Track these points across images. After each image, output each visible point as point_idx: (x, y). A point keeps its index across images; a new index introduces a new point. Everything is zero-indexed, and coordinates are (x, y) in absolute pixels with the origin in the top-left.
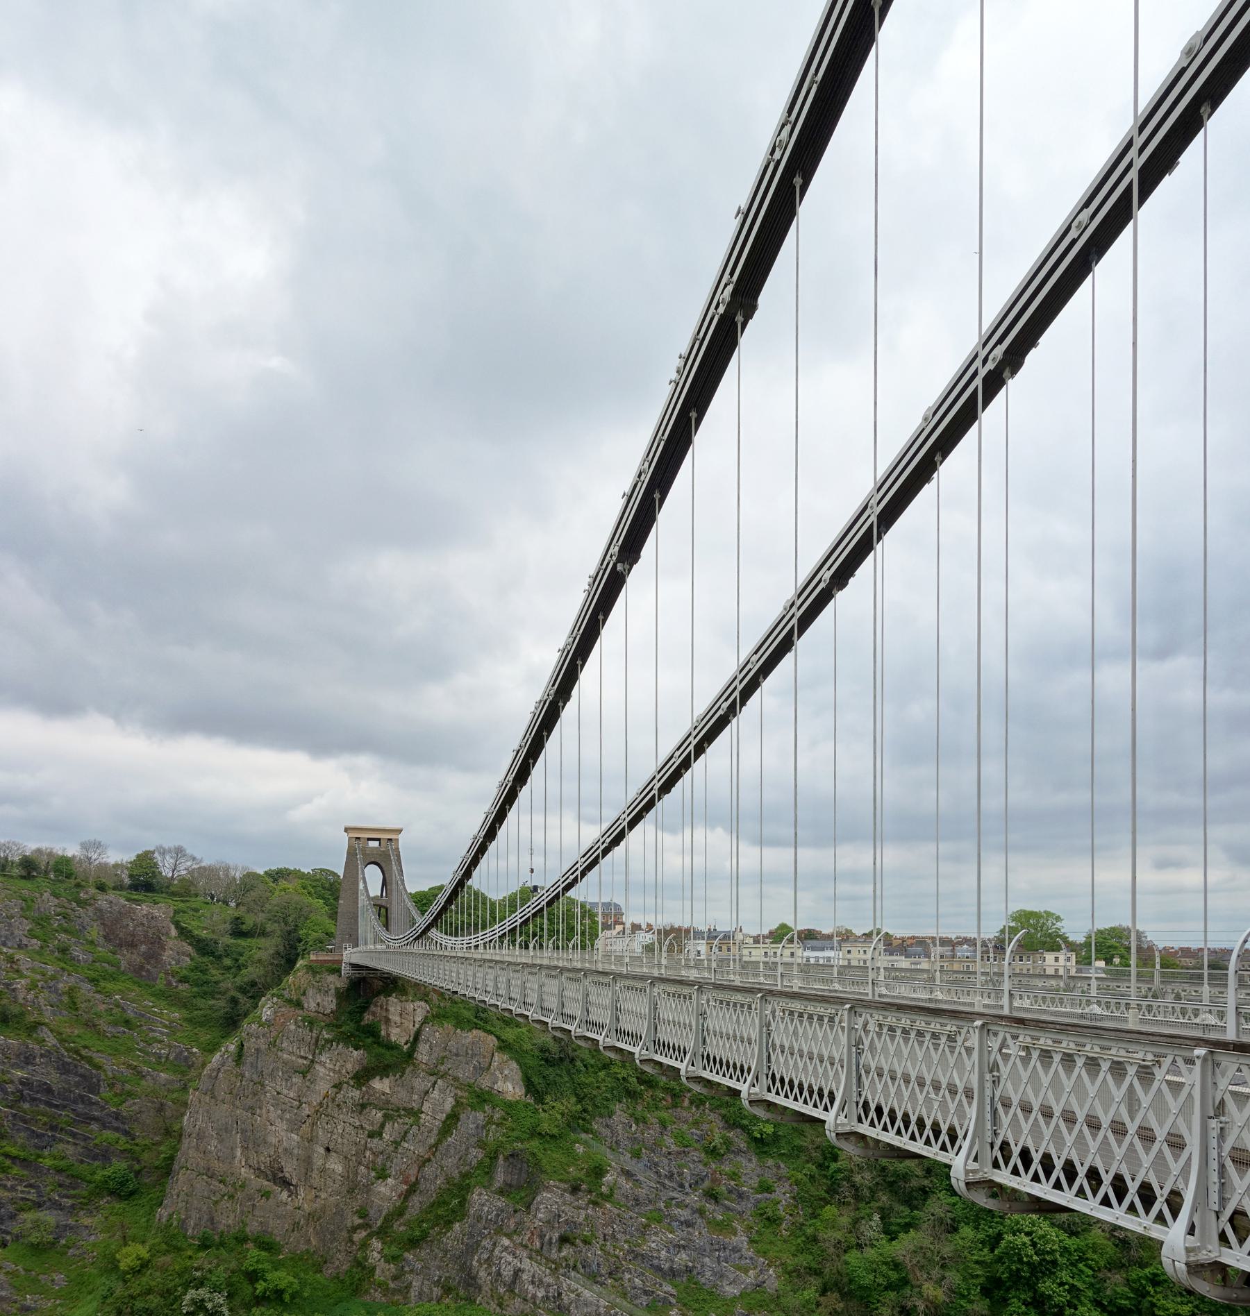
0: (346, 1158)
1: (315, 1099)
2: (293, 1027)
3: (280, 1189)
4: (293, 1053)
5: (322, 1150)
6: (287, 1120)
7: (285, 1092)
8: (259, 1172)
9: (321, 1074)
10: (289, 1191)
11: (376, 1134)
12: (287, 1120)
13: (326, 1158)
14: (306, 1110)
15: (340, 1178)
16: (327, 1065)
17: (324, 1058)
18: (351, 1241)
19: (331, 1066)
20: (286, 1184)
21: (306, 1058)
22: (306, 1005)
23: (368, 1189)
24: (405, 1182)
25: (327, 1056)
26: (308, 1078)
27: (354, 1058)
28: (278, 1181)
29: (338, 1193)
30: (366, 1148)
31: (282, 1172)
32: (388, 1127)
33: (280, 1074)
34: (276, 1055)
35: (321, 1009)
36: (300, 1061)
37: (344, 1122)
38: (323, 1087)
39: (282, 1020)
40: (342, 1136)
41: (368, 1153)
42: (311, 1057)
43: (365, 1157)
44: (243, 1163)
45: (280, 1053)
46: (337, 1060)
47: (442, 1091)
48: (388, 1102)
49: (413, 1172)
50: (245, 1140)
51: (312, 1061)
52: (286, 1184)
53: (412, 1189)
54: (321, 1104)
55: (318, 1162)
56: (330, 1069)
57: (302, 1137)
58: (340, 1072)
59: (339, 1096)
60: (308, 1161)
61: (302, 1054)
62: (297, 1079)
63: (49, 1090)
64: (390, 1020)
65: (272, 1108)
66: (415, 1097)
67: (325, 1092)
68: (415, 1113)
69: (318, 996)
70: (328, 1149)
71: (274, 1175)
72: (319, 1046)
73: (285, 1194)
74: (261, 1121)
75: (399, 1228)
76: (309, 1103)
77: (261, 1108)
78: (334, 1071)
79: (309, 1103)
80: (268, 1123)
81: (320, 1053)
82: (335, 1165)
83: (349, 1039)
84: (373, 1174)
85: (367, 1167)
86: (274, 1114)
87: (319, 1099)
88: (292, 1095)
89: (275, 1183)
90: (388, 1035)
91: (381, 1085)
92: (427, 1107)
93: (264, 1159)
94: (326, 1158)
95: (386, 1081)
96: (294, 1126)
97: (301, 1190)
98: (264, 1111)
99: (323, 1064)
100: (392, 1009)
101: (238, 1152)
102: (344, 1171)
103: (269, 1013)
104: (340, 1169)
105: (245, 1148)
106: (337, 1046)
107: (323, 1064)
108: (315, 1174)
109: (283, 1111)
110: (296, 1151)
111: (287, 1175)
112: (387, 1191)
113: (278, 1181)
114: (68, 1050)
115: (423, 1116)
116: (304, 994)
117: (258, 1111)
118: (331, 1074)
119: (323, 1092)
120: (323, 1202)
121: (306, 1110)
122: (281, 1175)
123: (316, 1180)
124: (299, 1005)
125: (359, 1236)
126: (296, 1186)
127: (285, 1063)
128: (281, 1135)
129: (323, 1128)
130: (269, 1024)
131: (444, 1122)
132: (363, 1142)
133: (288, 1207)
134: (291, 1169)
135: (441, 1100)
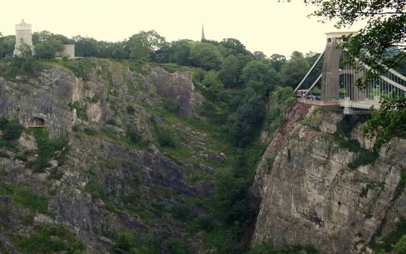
0: (350, 207)
1: (331, 177)
2: (317, 141)
4: (318, 154)
5: (336, 204)
6: (317, 188)
7: (316, 174)
8: (303, 215)
9: (333, 165)
10: (320, 224)
11: (364, 193)
12: (317, 188)
13: (339, 208)
14: (327, 184)
16: (336, 160)
17: (335, 156)
18: (356, 248)
19: (338, 161)
20: (318, 221)
21: (324, 157)
23: (362, 223)
26: (327, 167)
27: (349, 156)
28: (313, 220)
29: (347, 225)
31: (316, 215)
32: (369, 191)
33: (313, 165)
34: (310, 155)
35: (329, 132)
36: (321, 158)
38: (335, 171)
40: (347, 196)
42: (327, 156)
45: (312, 155)
46: (341, 158)
47: (395, 172)
48: (367, 179)
49: (383, 214)
50: (296, 199)
51: (328, 158)
52: (318, 221)
53: (384, 221)
55: (335, 209)
56: (338, 162)
58: (342, 164)
59: (344, 176)
60: (329, 211)
61: (323, 154)
62: (321, 168)
63: (161, 177)
65: (309, 183)
66: (381, 176)
67: (336, 174)
68: (382, 185)
69: (328, 125)
70: (339, 203)
71: (311, 217)
72: (330, 151)
73: (317, 227)
75: (379, 241)
77: (303, 183)
78: (339, 163)
80: (307, 191)
81: (333, 154)
82: (345, 211)
83: (344, 145)
84: (364, 215)
85: (360, 212)
86: (311, 185)
87: (333, 177)
88: (319, 176)
89: (312, 221)
90: (364, 144)
91: (363, 170)
92: (387, 181)
93: (306, 209)
94: (339, 208)
95: (366, 167)
96: (322, 191)
97: (326, 224)
98: (305, 184)
99: (334, 160)
101: (293, 205)
103: (303, 134)
104: (347, 213)
105: (296, 204)
106: (341, 150)
107: (334, 160)
108: (334, 217)
109: (316, 184)
110: (323, 204)
111: (319, 216)
112: (371, 223)
113: (313, 220)
114: (164, 155)
115: (386, 186)
116: (321, 124)
117: (302, 184)
118: (339, 165)
120: (338, 230)
122: (315, 216)
123: (334, 218)
124: (318, 130)
125: (360, 247)
126: (323, 222)
127: (315, 160)
128: (315, 197)
130: (304, 139)
131: (397, 189)
132: (357, 199)
133: (320, 233)
134: (320, 213)
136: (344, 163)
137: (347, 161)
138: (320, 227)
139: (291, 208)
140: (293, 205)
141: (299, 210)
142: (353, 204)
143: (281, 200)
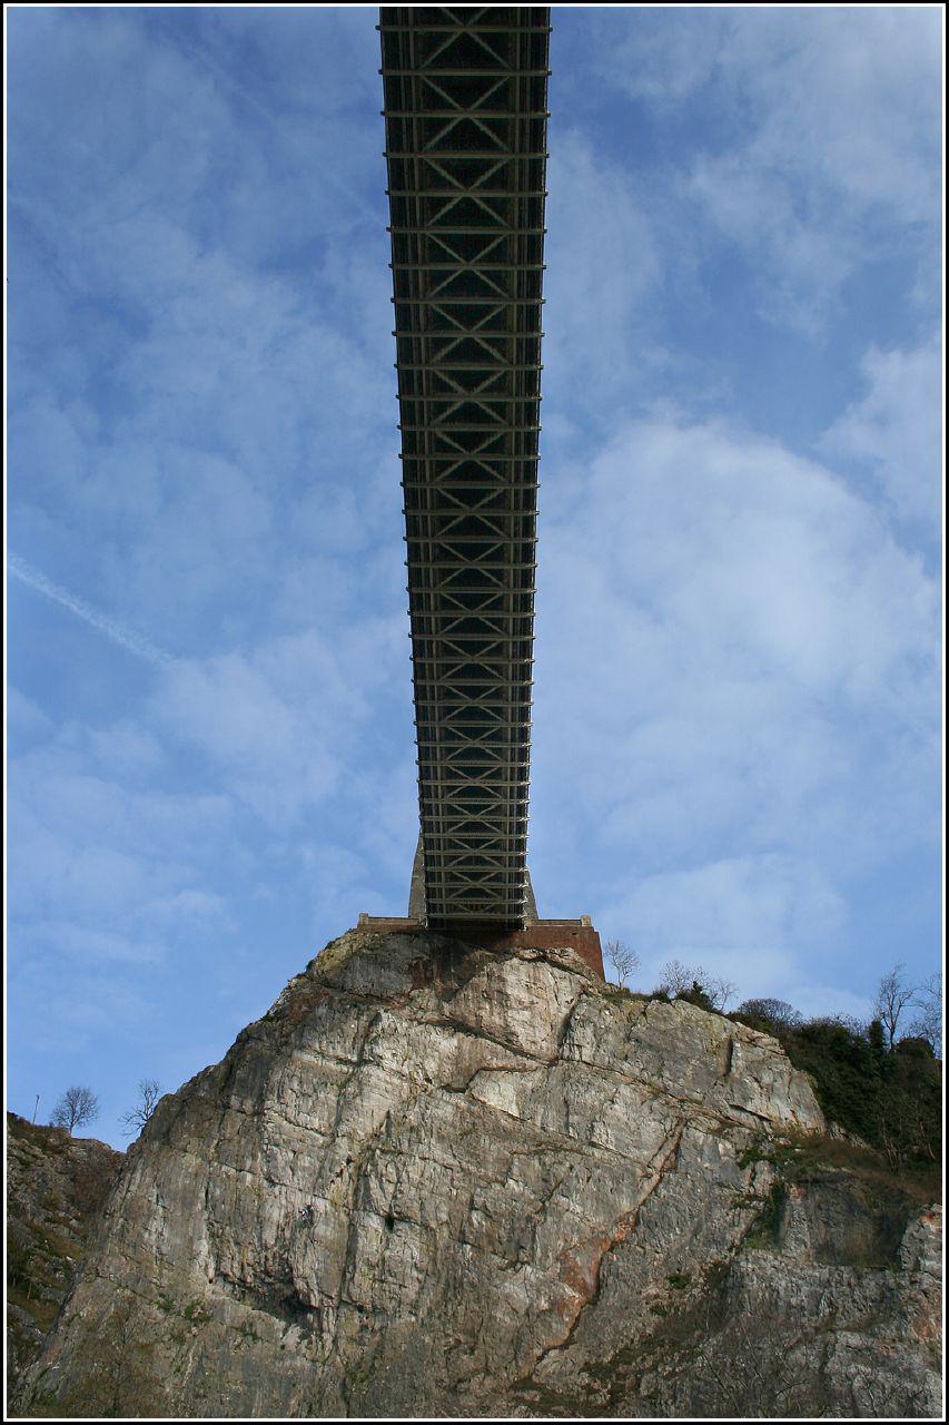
3: (283, 1324)
8: (243, 1289)
9: (373, 1080)
14: (343, 1149)
15: (415, 1274)
19: (394, 1066)
20: (295, 1307)
22: (349, 985)
24: (569, 1274)
25: (386, 1045)
30: (472, 1207)
36: (332, 1065)
37: (424, 1159)
39: (304, 1008)
41: (476, 1217)
43: (471, 1224)
44: (211, 1272)
49: (584, 1263)
52: (295, 1307)
54: (376, 1136)
57: (334, 1203)
64: (508, 996)
67: (383, 1113)
70: (390, 1222)
74: (253, 1181)
76: (350, 1136)
78: (401, 1075)
79: (350, 1136)
82: (409, 1248)
85: (477, 1248)
97: (330, 1322)
100: (511, 978)
102: (426, 1260)
117: (249, 1163)
118: (396, 1081)
119: (380, 1116)
121: (343, 1149)
126: (317, 1311)
129: (380, 1177)
135: (633, 1126)
136: (420, 1078)
137: (431, 1066)
138: (303, 1337)
139: (193, 1257)
140: (204, 1246)
141: (226, 1267)
142: (444, 1217)
143: (156, 1225)
